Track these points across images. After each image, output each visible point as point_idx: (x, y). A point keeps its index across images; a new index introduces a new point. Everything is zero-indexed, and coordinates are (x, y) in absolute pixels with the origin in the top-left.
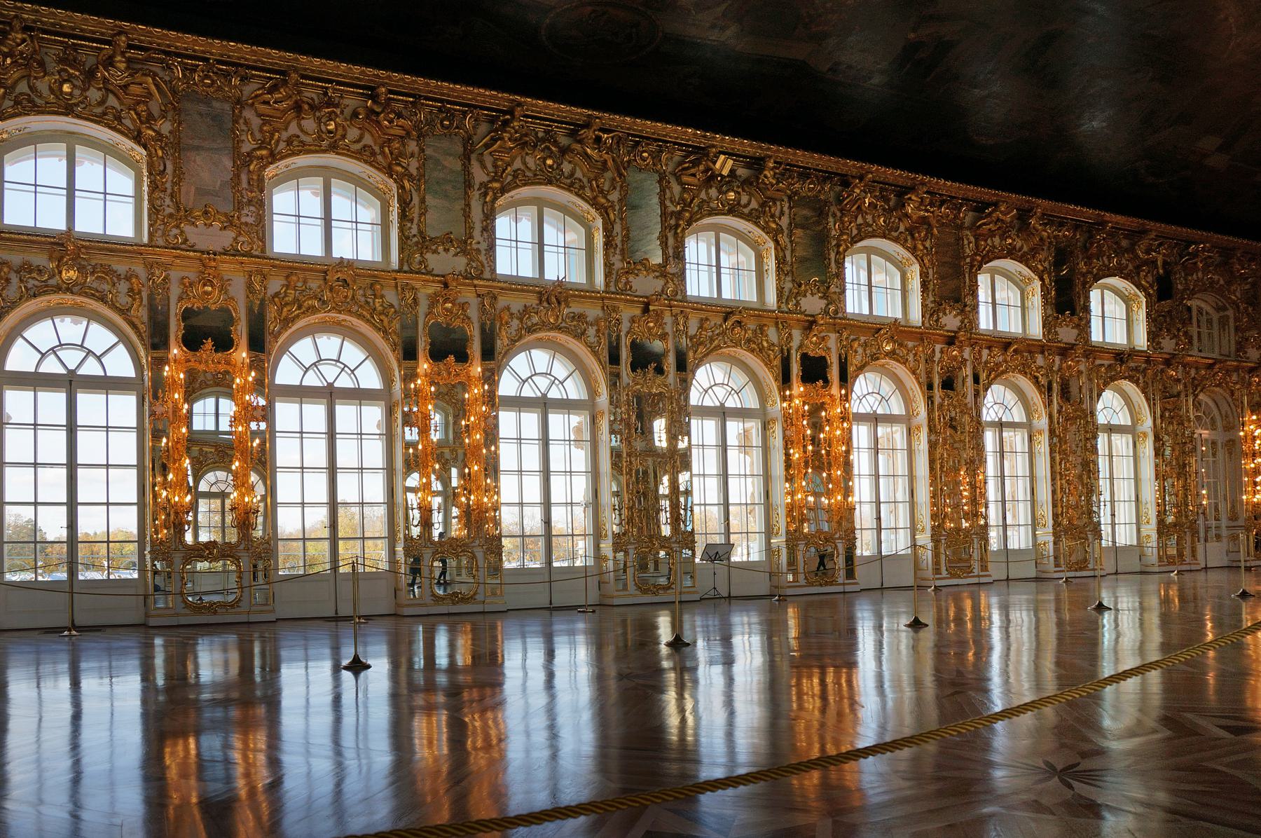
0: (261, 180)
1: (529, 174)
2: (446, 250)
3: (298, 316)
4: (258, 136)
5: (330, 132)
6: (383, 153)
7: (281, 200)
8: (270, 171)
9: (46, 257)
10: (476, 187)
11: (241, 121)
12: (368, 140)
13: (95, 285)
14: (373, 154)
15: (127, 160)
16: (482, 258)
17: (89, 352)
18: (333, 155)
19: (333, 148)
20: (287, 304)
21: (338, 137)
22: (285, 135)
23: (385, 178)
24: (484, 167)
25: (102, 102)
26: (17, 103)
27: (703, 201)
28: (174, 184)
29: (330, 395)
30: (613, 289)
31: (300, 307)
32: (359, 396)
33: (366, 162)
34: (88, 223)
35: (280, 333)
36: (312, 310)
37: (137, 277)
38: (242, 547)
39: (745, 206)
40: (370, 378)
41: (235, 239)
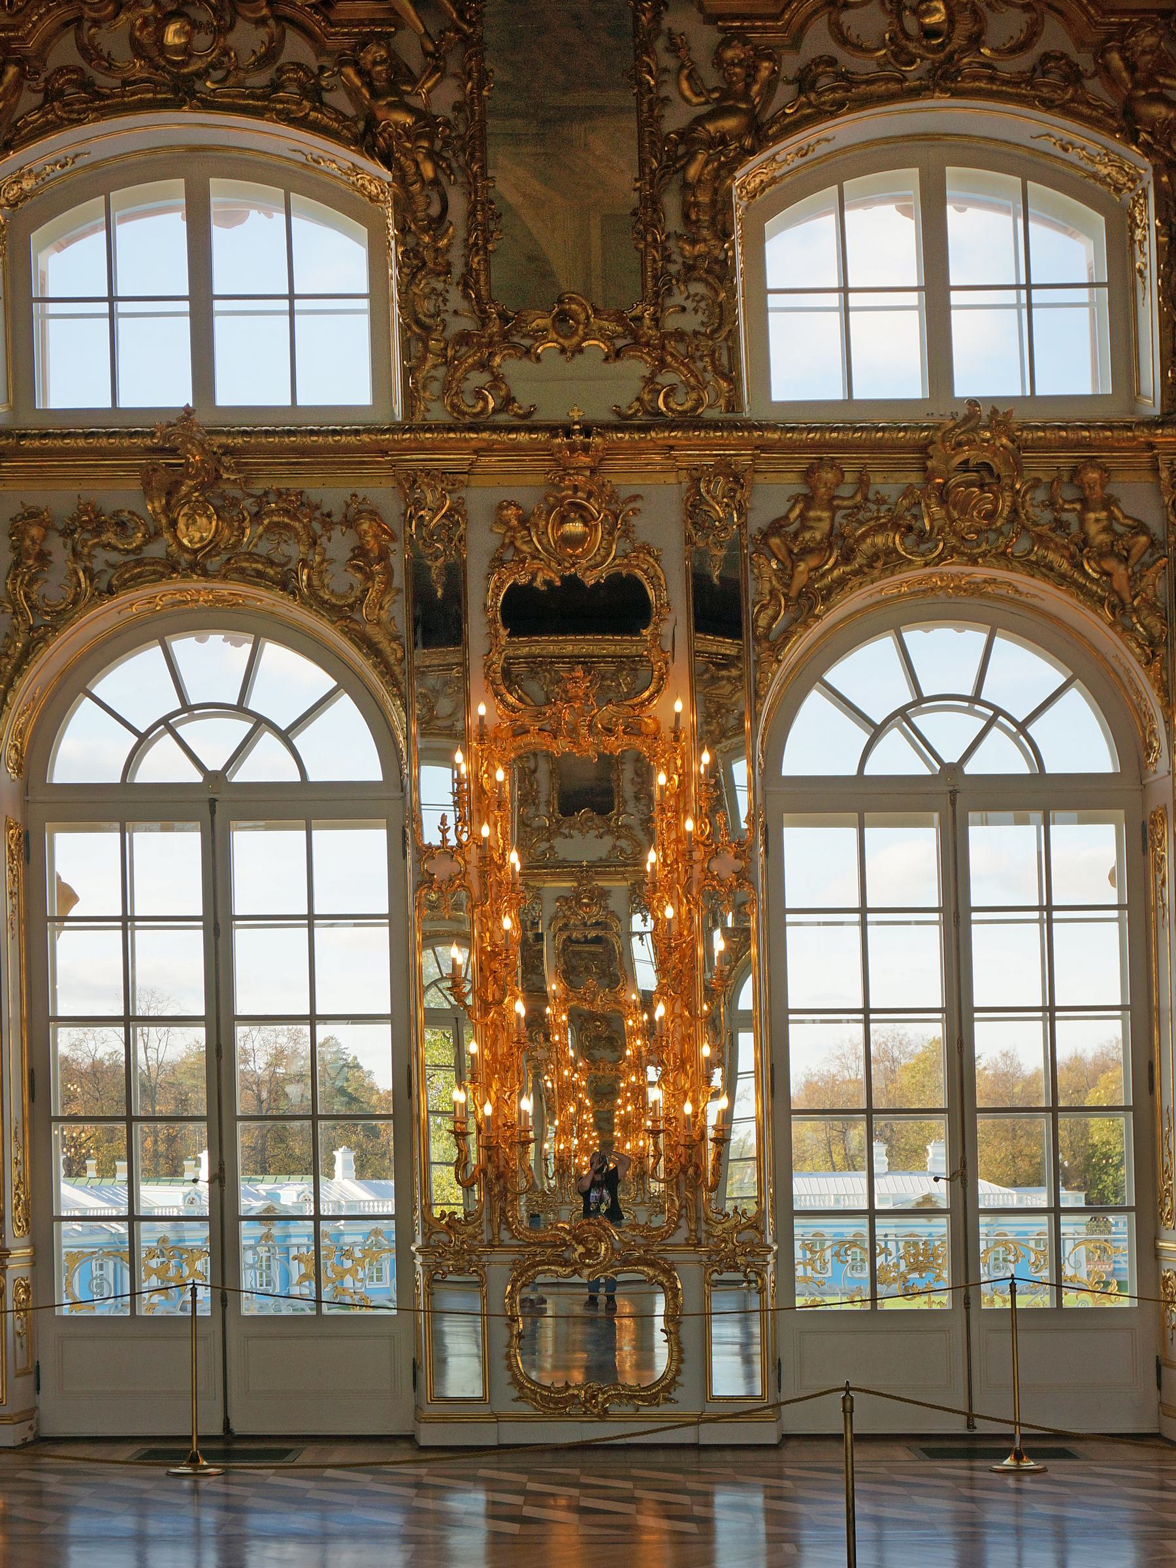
0: (721, 207)
3: (841, 582)
4: (712, 78)
5: (930, 32)
6: (1104, 69)
7: (794, 251)
8: (749, 175)
9: (136, 486)
11: (660, 44)
12: (1055, 37)
13: (263, 548)
14: (1074, 76)
15: (346, 202)
17: (261, 723)
18: (942, 101)
19: (945, 79)
20: (806, 551)
21: (958, 41)
22: (791, 64)
23: (1116, 144)
25: (268, 57)
26: (51, 96)
28: (471, 248)
29: (950, 801)
31: (847, 557)
32: (1042, 796)
33: (1048, 105)
34: (251, 378)
35: (786, 635)
36: (889, 561)
37: (374, 515)
38: (681, 1236)
40: (1078, 741)
41: (649, 381)
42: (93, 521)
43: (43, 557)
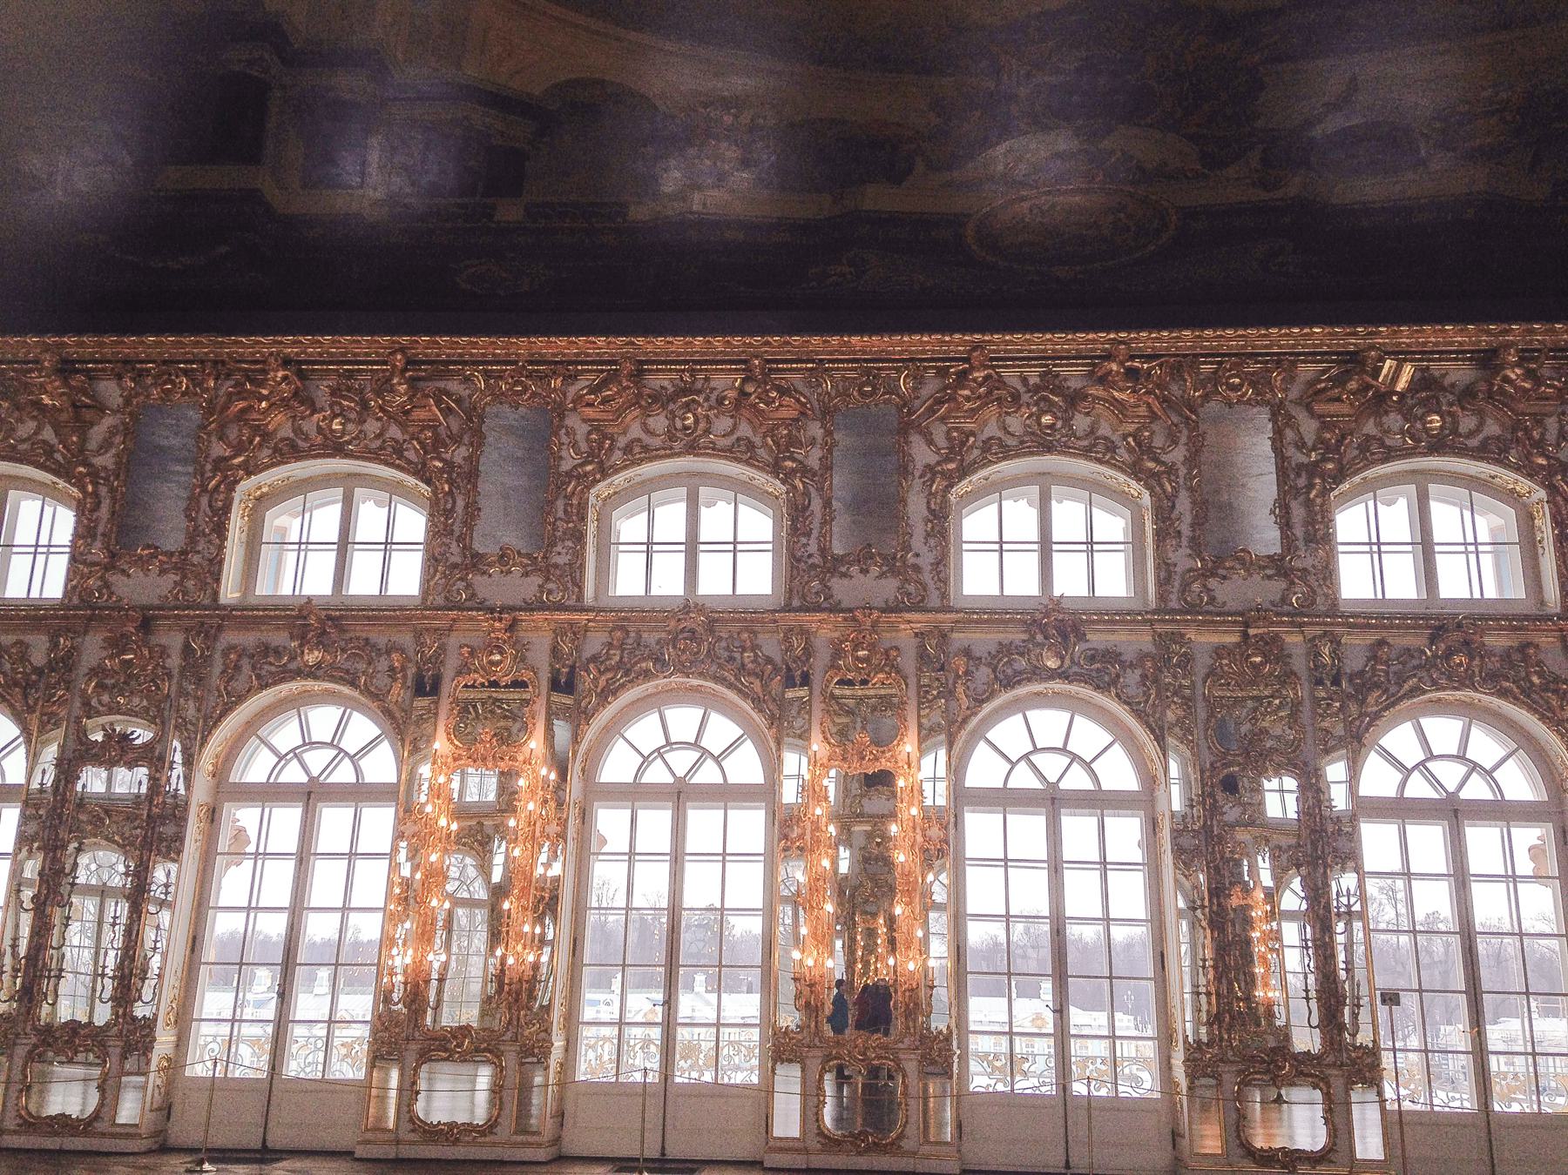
1: (1011, 442)
2: (865, 571)
3: (623, 686)
9: (286, 634)
10: (917, 474)
13: (347, 665)
16: (927, 577)
19: (692, 449)
20: (607, 670)
24: (930, 442)
26: (276, 450)
27: (1368, 438)
28: (465, 523)
30: (1174, 604)
31: (626, 674)
35: (595, 710)
36: (647, 675)
37: (402, 651)
39: (1471, 434)
42: (266, 650)
43: (237, 668)
